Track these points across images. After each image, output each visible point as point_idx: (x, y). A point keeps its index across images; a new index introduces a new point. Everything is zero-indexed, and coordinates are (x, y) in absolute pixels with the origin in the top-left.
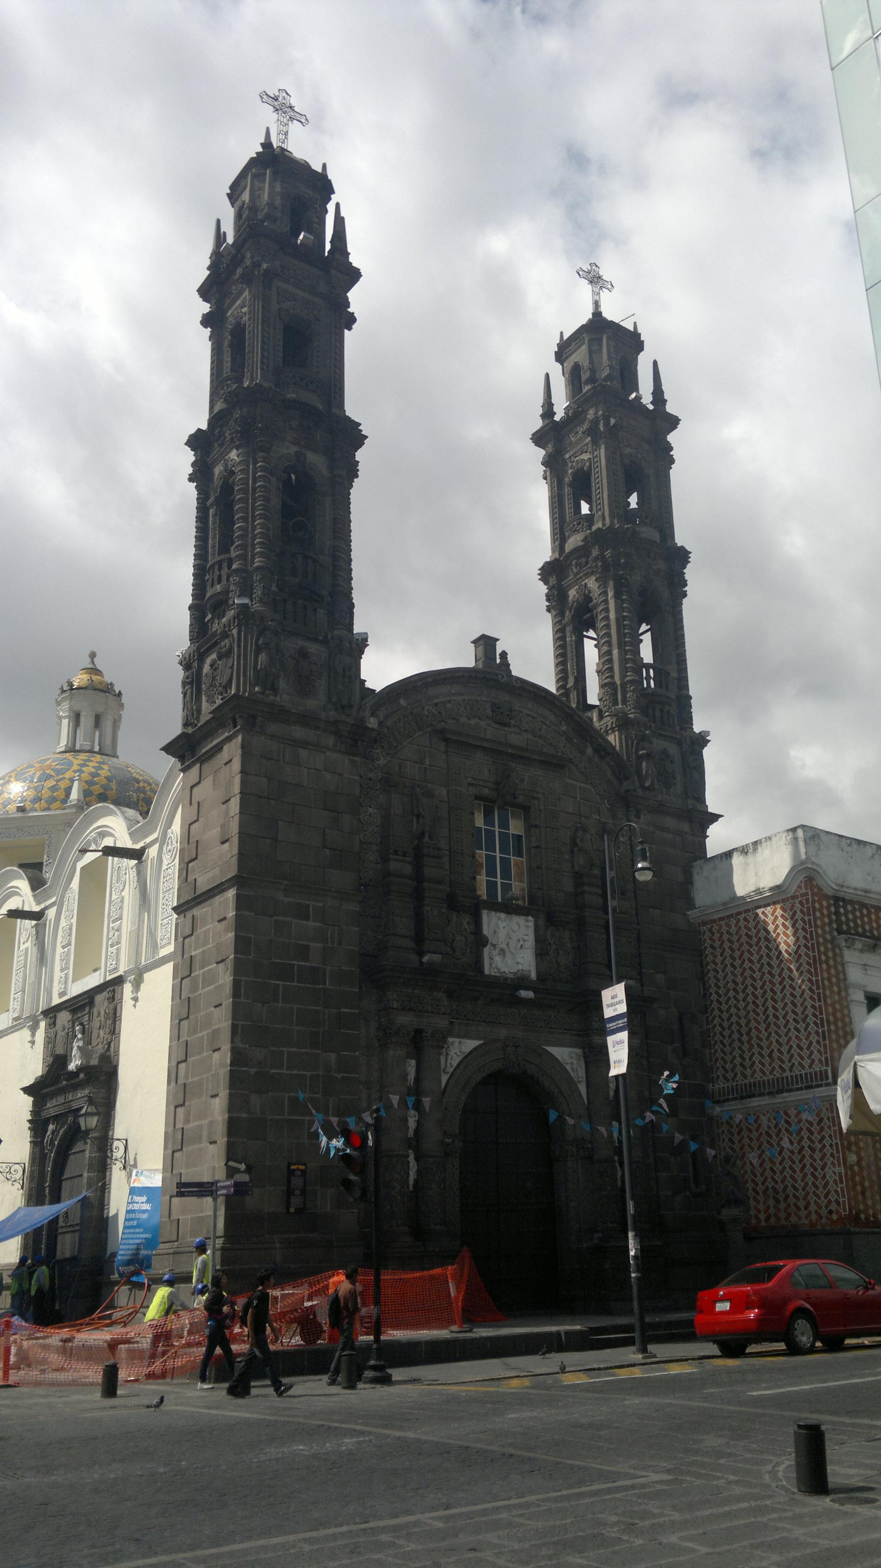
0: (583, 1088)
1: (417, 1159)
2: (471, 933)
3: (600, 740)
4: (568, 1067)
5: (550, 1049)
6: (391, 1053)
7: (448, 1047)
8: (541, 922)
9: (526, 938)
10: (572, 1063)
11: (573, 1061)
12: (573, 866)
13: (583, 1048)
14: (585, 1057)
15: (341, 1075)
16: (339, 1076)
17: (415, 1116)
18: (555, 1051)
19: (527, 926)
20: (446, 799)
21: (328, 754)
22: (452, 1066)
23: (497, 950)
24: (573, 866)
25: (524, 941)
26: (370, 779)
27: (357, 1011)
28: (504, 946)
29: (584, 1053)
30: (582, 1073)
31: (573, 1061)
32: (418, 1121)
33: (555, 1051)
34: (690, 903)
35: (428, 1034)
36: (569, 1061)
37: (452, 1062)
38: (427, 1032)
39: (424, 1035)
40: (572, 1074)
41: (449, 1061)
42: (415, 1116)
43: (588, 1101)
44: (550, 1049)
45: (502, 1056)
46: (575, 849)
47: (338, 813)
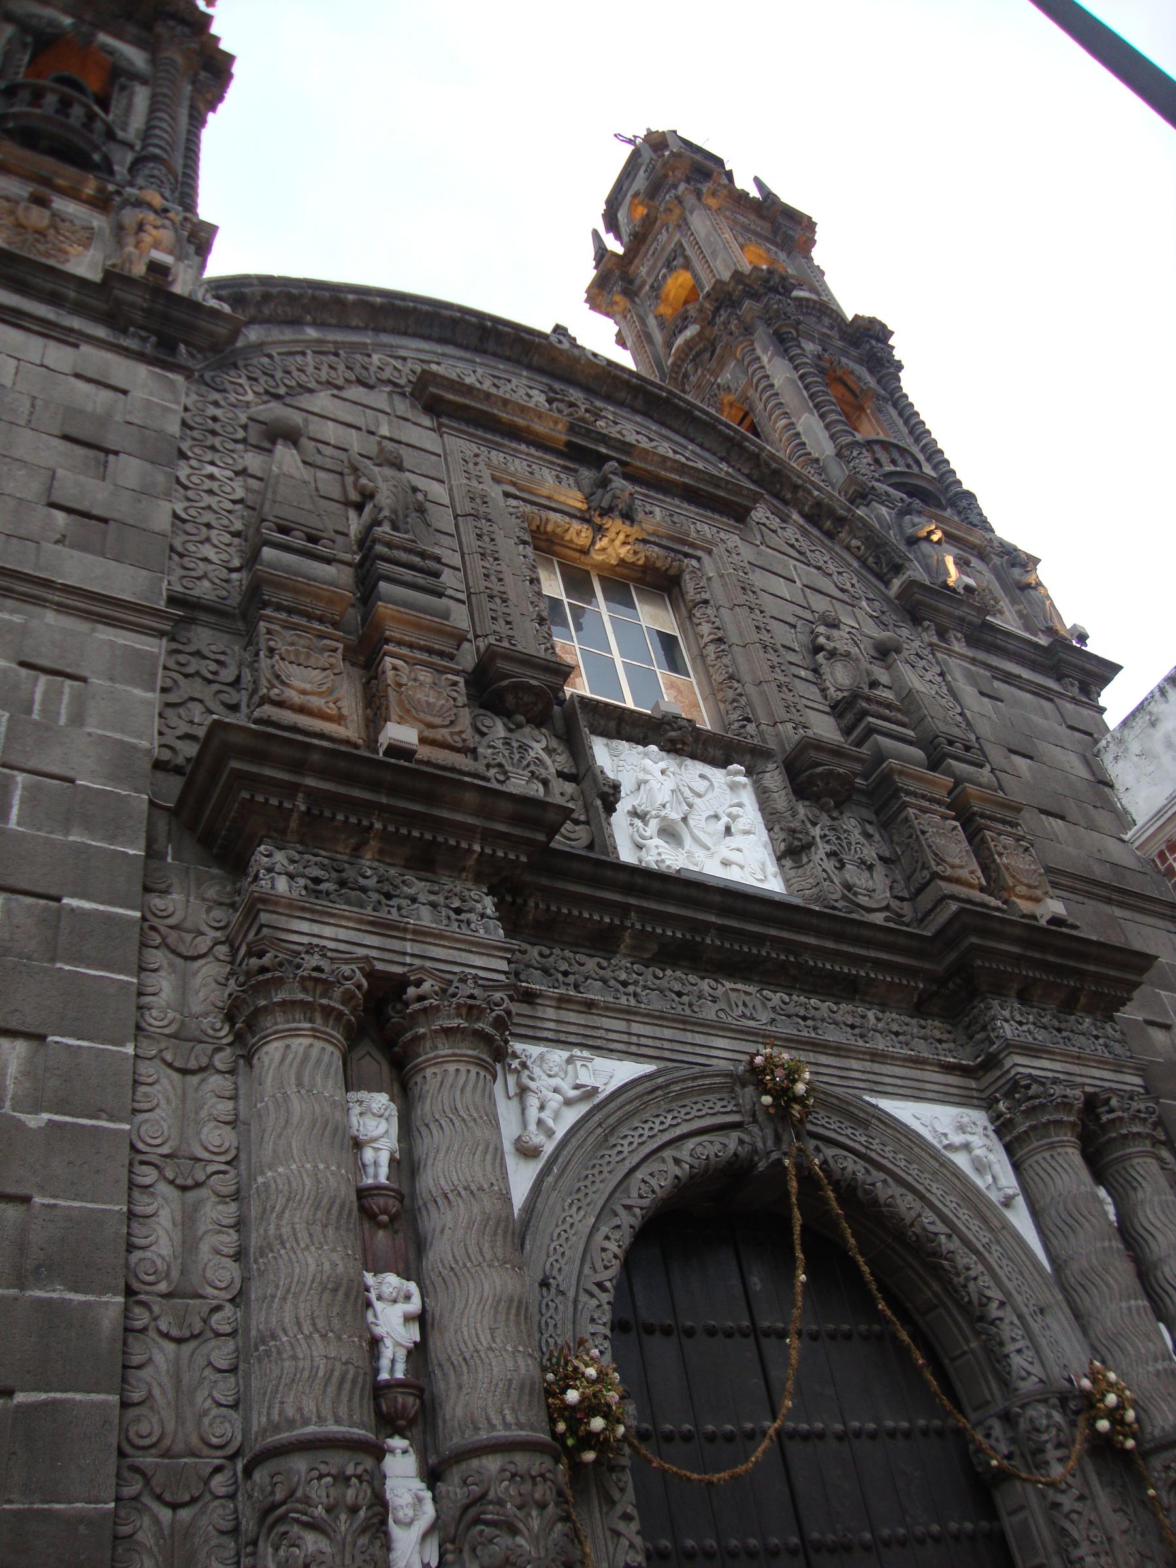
0: (1021, 1221)
1: (432, 1476)
2: (560, 774)
3: (816, 493)
4: (961, 1160)
5: (888, 1105)
6: (272, 1051)
7: (524, 1065)
8: (774, 778)
9: (735, 810)
10: (966, 1147)
11: (970, 1138)
12: (823, 690)
13: (988, 1104)
14: (1002, 1128)
15: (46, 1116)
16: (36, 1121)
17: (408, 1298)
18: (904, 1111)
19: (733, 787)
20: (447, 501)
21: (85, 348)
22: (550, 1133)
23: (654, 824)
24: (823, 690)
25: (734, 818)
26: (215, 419)
27: (138, 914)
28: (675, 816)
29: (995, 1118)
30: (1008, 1181)
31: (970, 1138)
32: (422, 1319)
33: (904, 1111)
34: (1123, 819)
35: (426, 986)
36: (957, 1139)
37: (546, 1116)
38: (418, 983)
39: (412, 991)
40: (980, 1183)
41: (533, 1113)
42: (408, 1298)
43: (1052, 1259)
44: (886, 1104)
45: (736, 1118)
46: (820, 657)
47: (108, 452)
